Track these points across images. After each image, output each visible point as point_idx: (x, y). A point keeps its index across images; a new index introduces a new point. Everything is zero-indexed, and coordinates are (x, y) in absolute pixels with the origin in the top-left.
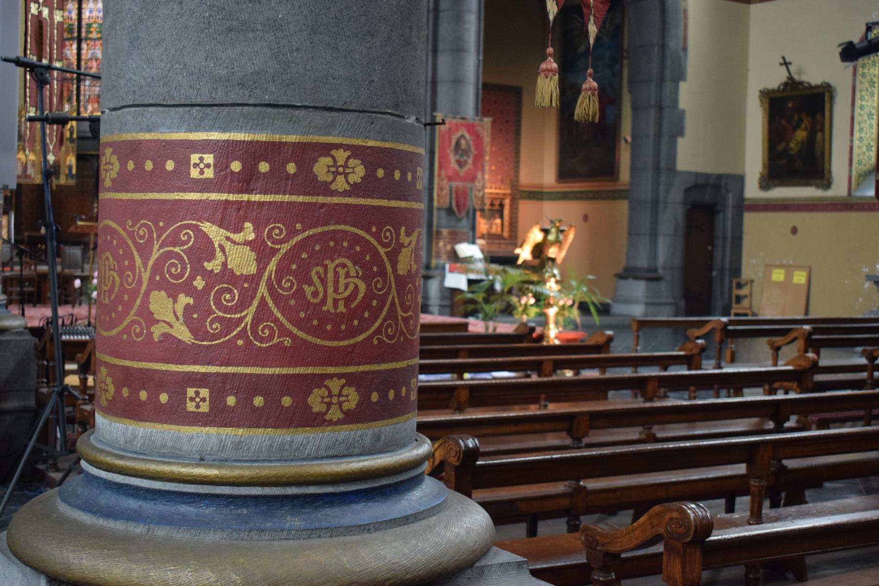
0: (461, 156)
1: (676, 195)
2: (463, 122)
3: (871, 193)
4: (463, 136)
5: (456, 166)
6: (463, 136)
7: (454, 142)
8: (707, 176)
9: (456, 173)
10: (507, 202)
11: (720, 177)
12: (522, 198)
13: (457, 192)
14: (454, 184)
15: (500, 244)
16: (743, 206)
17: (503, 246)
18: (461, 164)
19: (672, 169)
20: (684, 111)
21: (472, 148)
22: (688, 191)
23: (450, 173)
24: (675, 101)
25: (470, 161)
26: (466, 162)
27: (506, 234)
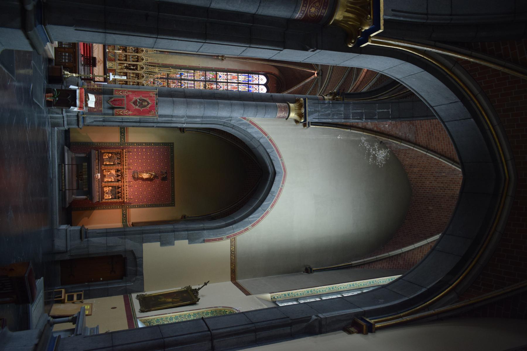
0: (139, 102)
1: (129, 244)
2: (155, 104)
3: (140, 325)
4: (148, 104)
5: (134, 100)
6: (148, 104)
7: (145, 99)
8: (141, 265)
9: (131, 100)
10: (120, 200)
11: (142, 274)
12: (123, 211)
13: (121, 100)
14: (125, 98)
15: (99, 192)
16: (126, 293)
17: (98, 193)
18: (135, 103)
19: (143, 241)
20: (174, 245)
21: (143, 109)
22: (132, 252)
23: (130, 96)
24: (178, 239)
25: (137, 107)
26: (137, 105)
27: (104, 200)
